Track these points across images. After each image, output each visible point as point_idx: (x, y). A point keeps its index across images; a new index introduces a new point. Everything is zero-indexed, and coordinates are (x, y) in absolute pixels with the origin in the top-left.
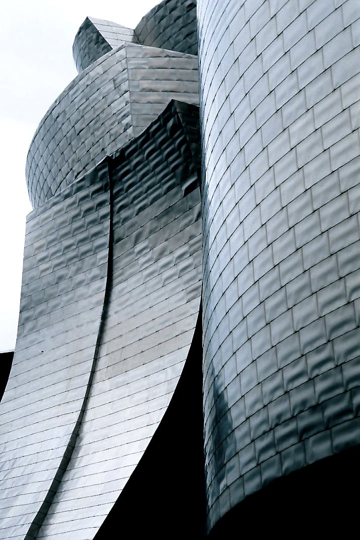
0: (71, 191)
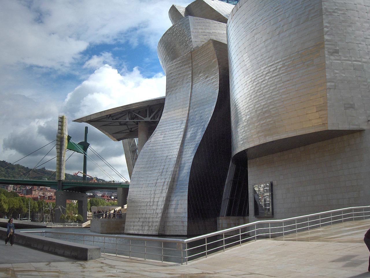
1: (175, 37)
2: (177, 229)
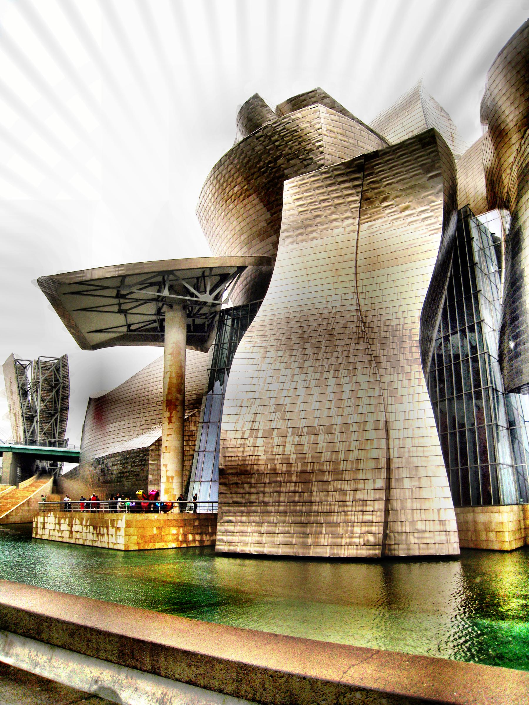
0: (329, 170)
1: (277, 144)
2: (428, 541)
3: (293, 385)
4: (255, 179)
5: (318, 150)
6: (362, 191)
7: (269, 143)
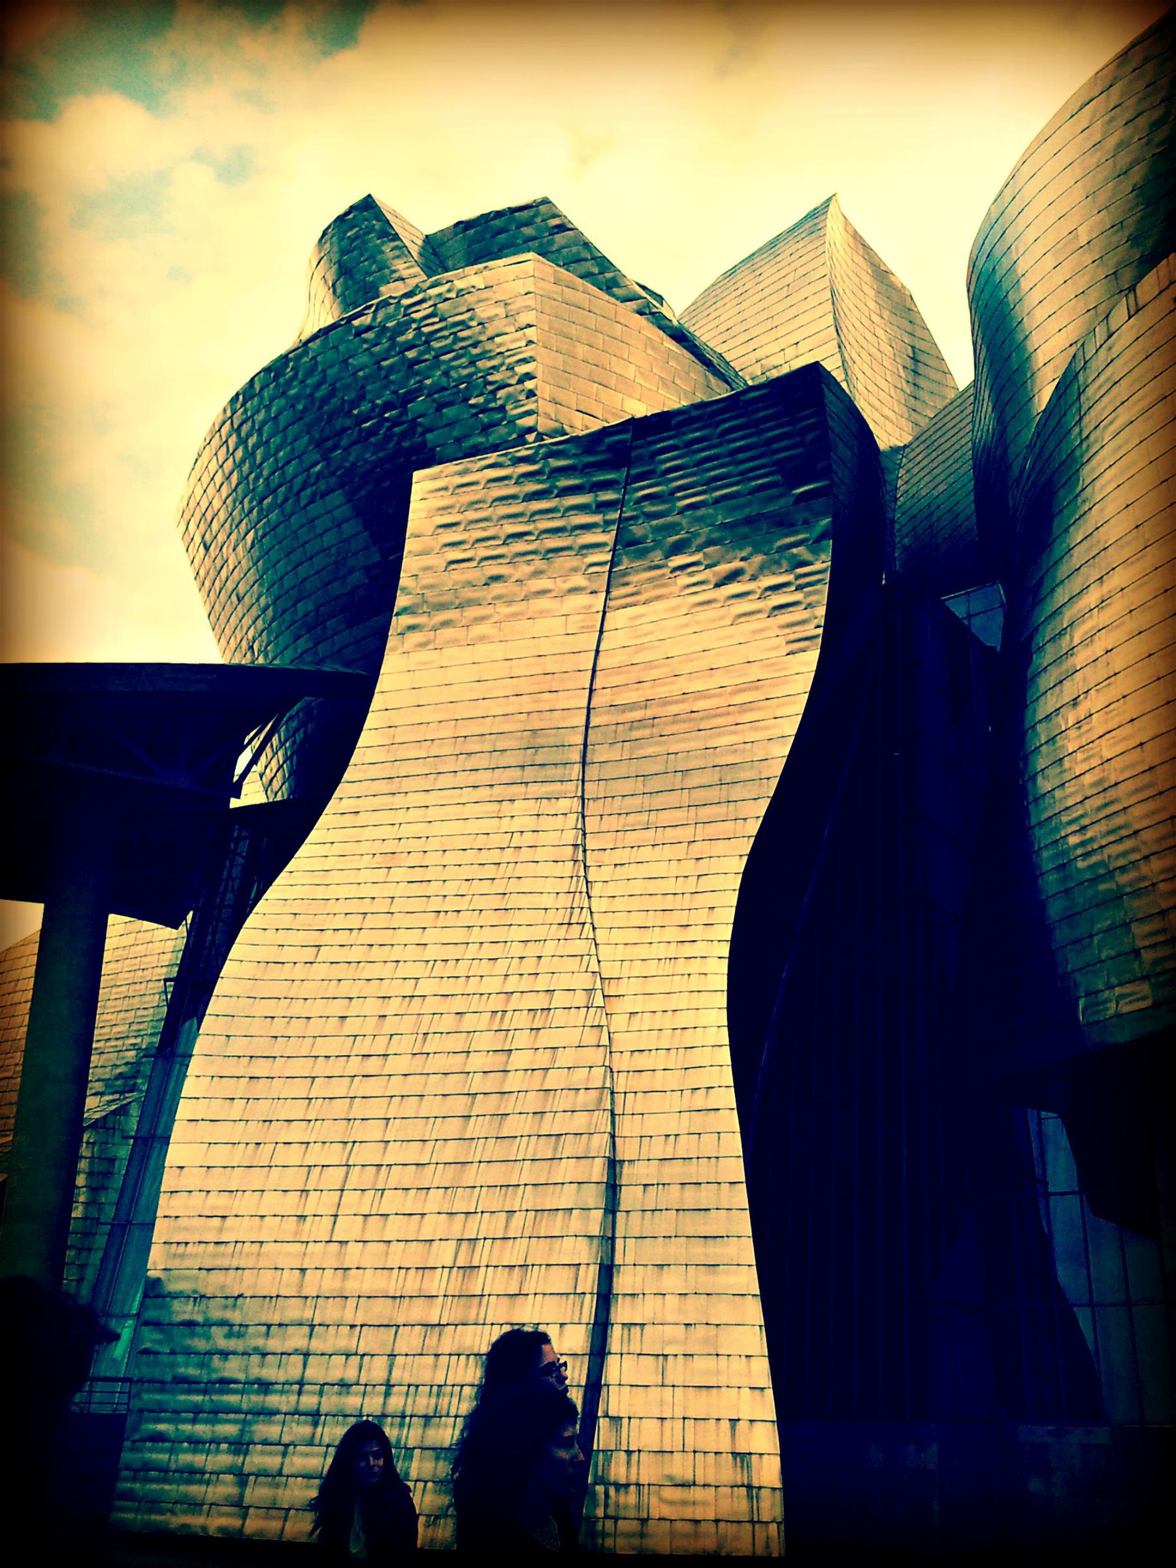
0: (536, 453)
1: (411, 354)
3: (379, 1047)
4: (345, 449)
5: (519, 387)
6: (620, 520)
7: (389, 350)
